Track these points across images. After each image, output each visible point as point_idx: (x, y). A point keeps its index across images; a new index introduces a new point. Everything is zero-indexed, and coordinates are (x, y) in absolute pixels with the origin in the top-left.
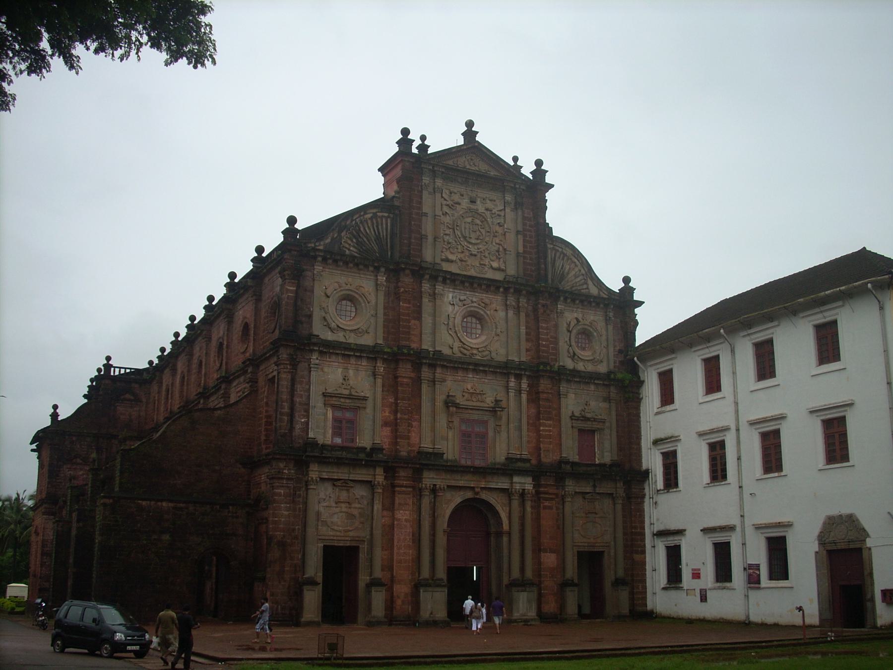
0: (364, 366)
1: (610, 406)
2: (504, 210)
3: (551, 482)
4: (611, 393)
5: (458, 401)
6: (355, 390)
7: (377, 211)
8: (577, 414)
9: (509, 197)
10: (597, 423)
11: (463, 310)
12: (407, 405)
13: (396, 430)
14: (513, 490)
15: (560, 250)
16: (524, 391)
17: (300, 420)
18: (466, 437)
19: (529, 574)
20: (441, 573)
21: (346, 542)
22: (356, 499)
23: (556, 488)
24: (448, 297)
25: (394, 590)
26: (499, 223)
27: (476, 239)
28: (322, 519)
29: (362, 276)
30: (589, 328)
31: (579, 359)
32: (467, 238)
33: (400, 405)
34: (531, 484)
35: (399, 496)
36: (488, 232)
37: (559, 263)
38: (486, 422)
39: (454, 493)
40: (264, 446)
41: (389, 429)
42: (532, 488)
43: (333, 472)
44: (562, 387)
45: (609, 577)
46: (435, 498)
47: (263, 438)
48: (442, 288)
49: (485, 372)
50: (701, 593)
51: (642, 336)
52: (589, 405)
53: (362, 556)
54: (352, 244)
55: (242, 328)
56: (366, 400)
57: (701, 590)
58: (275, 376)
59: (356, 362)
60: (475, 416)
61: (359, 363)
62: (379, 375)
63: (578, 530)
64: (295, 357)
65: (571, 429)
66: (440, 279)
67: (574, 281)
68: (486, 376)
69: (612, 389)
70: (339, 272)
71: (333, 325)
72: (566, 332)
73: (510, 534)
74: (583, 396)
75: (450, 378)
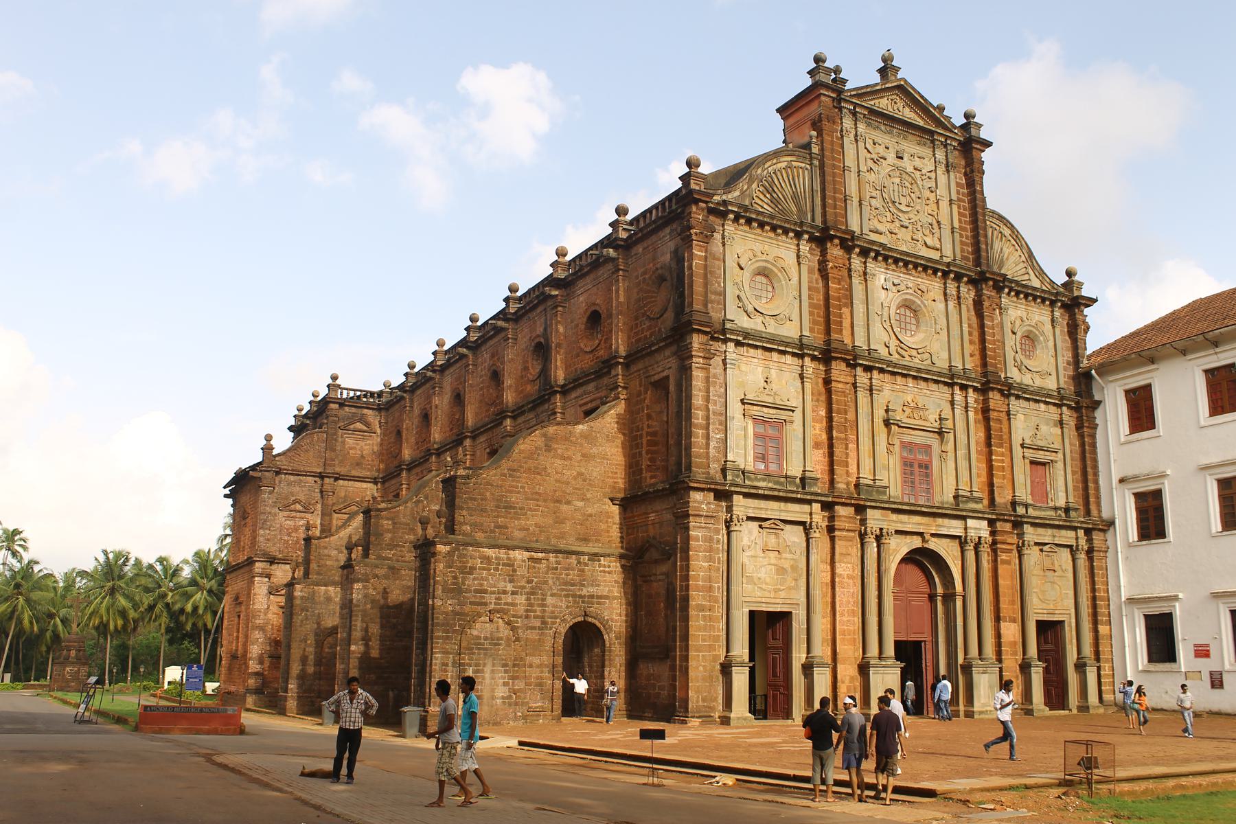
1: (1062, 433)
2: (935, 170)
3: (1008, 527)
5: (898, 419)
7: (792, 159)
8: (1027, 441)
9: (940, 155)
13: (831, 454)
15: (998, 228)
18: (907, 464)
20: (890, 650)
21: (776, 606)
24: (879, 281)
29: (780, 243)
30: (1034, 330)
32: (897, 204)
33: (835, 419)
36: (919, 198)
37: (997, 245)
38: (930, 446)
40: (649, 474)
45: (1071, 657)
46: (879, 547)
47: (645, 463)
49: (926, 380)
50: (1211, 678)
51: (1094, 342)
54: (766, 200)
55: (585, 320)
57: (1211, 673)
58: (668, 377)
59: (778, 358)
60: (917, 438)
62: (807, 378)
64: (709, 347)
66: (872, 254)
67: (1015, 270)
69: (1064, 408)
70: (753, 236)
71: (750, 309)
72: (1010, 333)
75: (887, 387)
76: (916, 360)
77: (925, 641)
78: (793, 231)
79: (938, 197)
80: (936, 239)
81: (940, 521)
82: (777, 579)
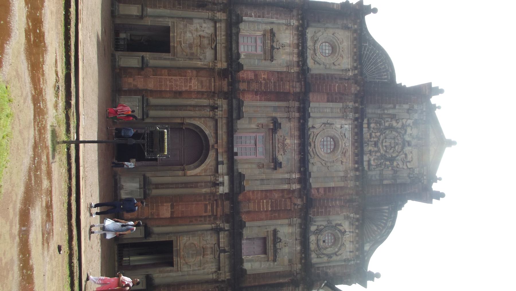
0: (293, 59)
4: (296, 265)
6: (276, 51)
10: (272, 254)
11: (339, 135)
12: (271, 89)
14: (218, 176)
16: (290, 187)
17: (253, 12)
19: (155, 192)
21: (173, 42)
22: (204, 50)
23: (222, 214)
25: (140, 76)
26: (398, 164)
28: (188, 25)
31: (317, 235)
34: (223, 191)
35: (208, 81)
39: (212, 127)
41: (253, 77)
42: (220, 192)
43: (221, 32)
44: (297, 220)
49: (300, 153)
52: (285, 246)
53: (164, 55)
56: (271, 60)
61: (295, 56)
63: (190, 240)
65: (266, 230)
66: (357, 115)
68: (296, 155)
73: (184, 176)
74: (291, 240)
76: (309, 148)
77: (157, 161)
78: (357, 65)
81: (225, 156)
82: (187, 44)
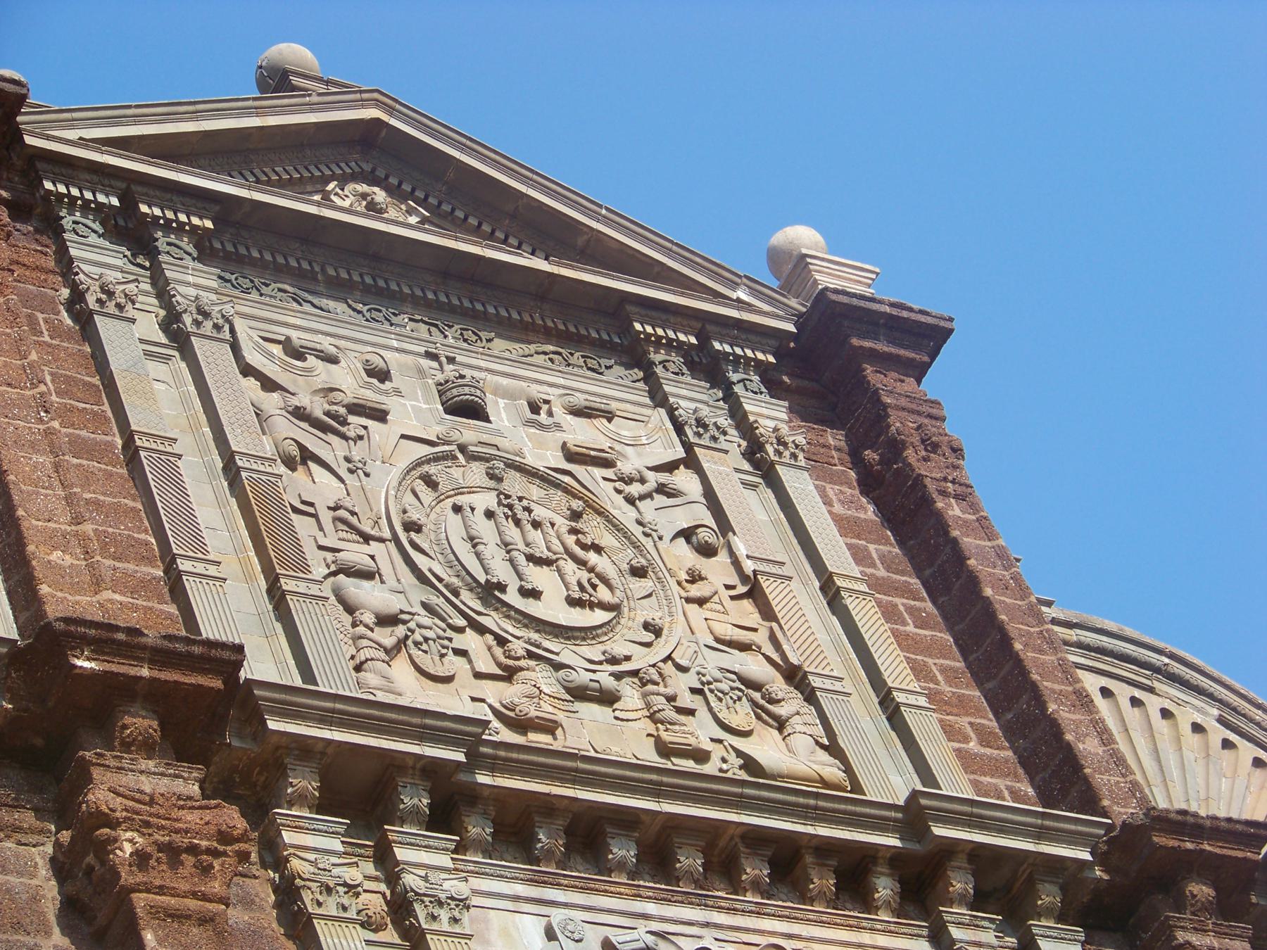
2: (691, 462)
26: (687, 534)
27: (573, 602)
36: (638, 572)
48: (445, 860)
79: (749, 566)
80: (802, 743)
